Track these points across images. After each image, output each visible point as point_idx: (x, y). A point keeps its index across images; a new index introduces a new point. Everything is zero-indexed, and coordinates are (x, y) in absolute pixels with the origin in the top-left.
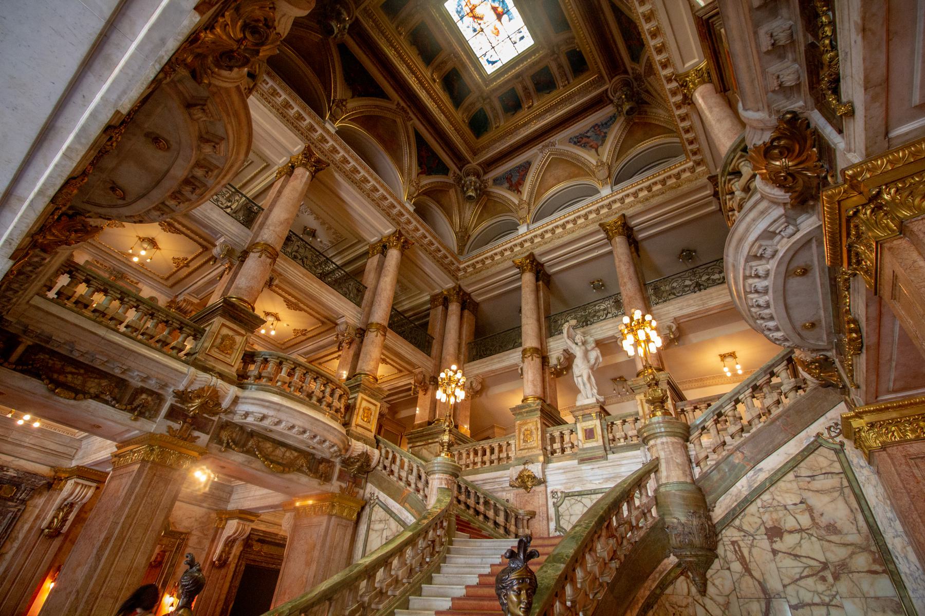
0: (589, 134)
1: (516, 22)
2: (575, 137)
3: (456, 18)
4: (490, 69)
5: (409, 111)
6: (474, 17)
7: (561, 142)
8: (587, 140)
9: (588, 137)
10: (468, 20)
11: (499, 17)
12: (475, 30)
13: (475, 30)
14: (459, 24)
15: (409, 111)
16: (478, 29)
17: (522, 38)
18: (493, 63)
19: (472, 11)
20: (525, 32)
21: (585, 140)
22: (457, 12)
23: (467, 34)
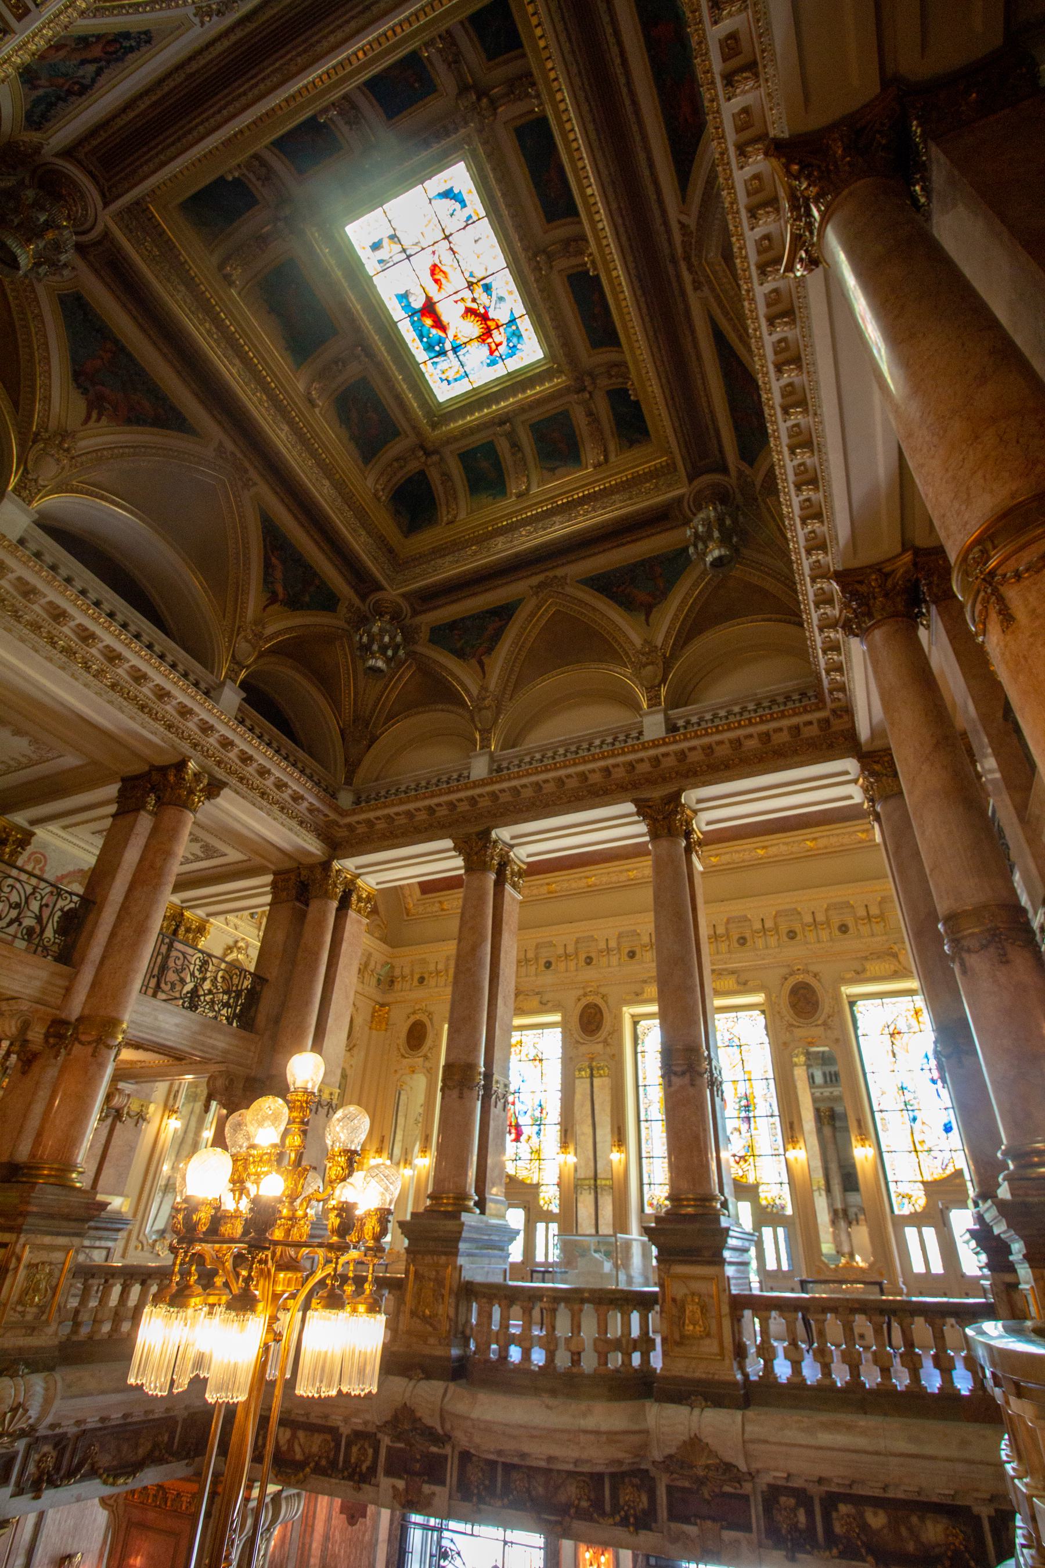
0: (91, 68)
1: (395, 286)
2: (131, 49)
3: (526, 325)
4: (458, 175)
5: (680, 250)
6: (484, 318)
7: (180, 27)
8: (89, 55)
9: (84, 62)
10: (499, 314)
11: (429, 309)
12: (487, 288)
13: (487, 288)
14: (520, 309)
15: (680, 250)
16: (479, 291)
17: (376, 246)
18: (447, 194)
19: (488, 333)
20: (370, 262)
21: (97, 51)
22: (520, 336)
23: (505, 284)
